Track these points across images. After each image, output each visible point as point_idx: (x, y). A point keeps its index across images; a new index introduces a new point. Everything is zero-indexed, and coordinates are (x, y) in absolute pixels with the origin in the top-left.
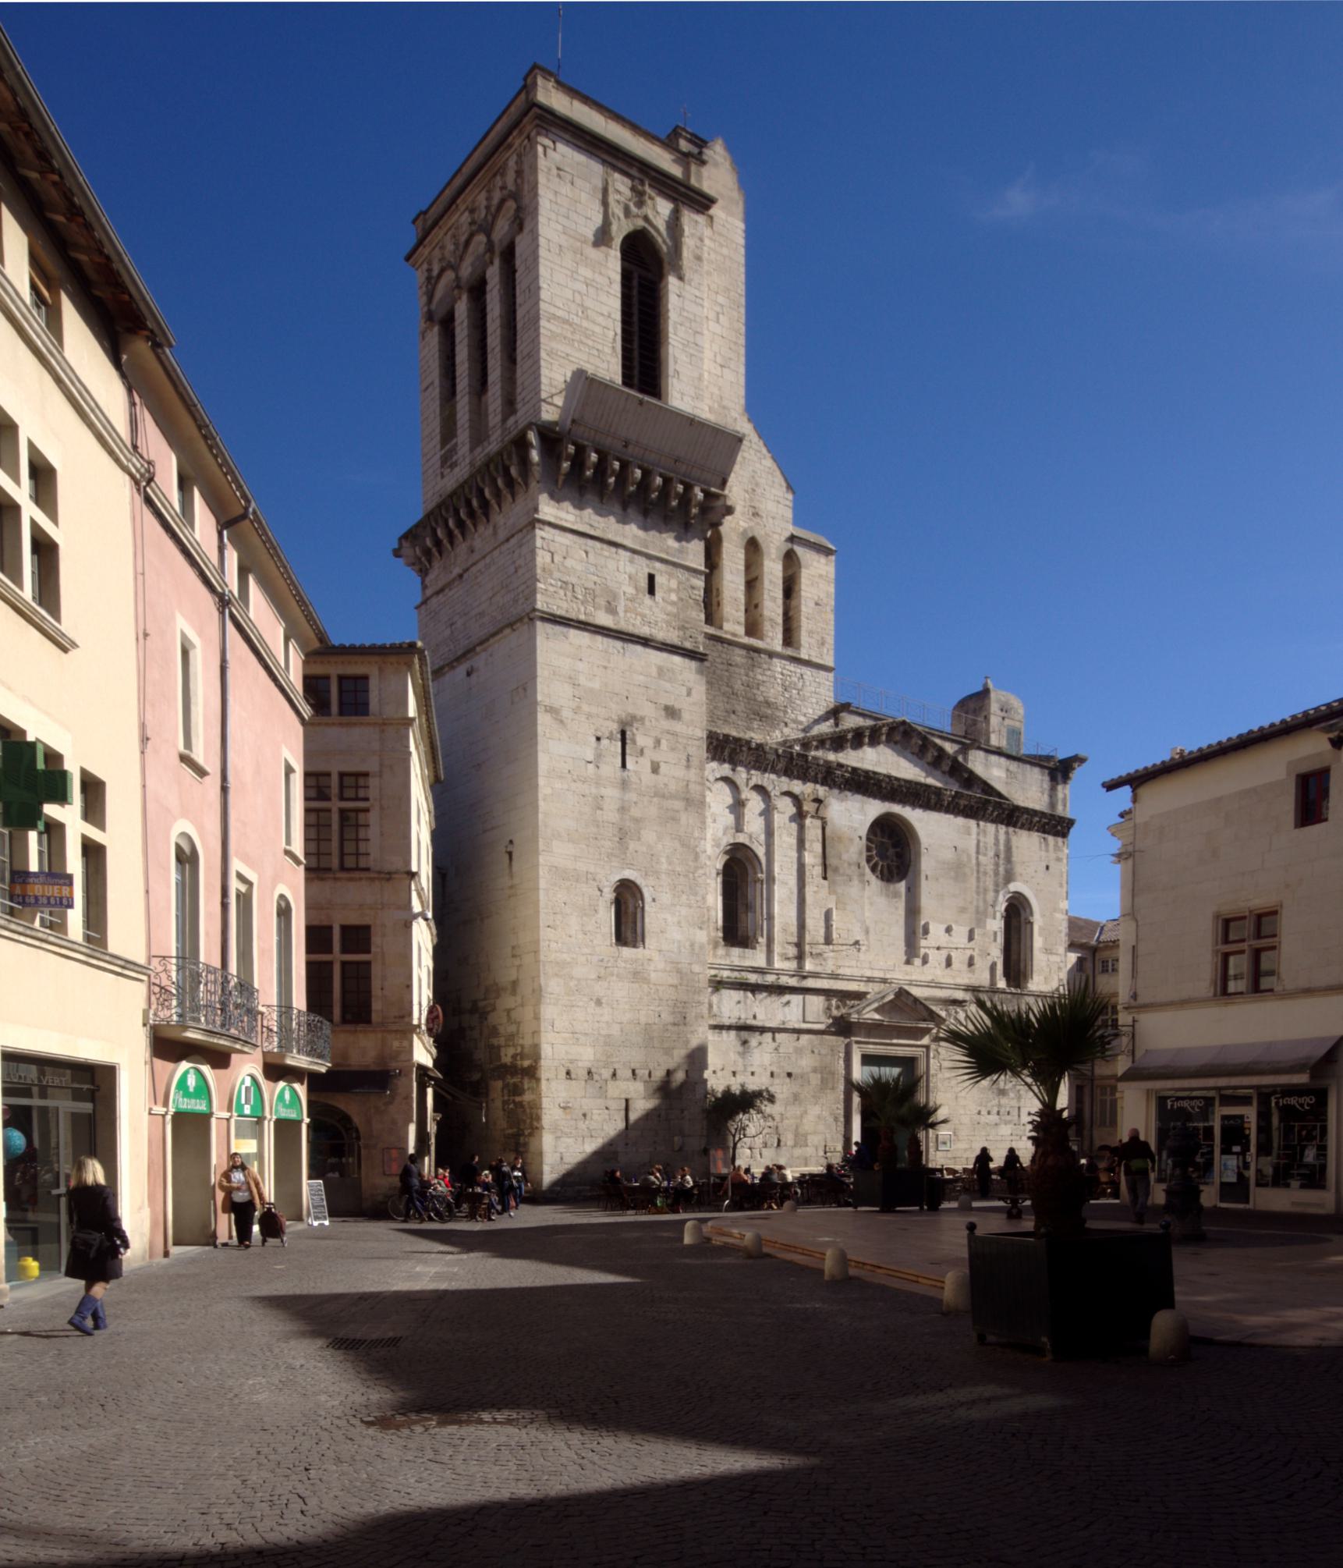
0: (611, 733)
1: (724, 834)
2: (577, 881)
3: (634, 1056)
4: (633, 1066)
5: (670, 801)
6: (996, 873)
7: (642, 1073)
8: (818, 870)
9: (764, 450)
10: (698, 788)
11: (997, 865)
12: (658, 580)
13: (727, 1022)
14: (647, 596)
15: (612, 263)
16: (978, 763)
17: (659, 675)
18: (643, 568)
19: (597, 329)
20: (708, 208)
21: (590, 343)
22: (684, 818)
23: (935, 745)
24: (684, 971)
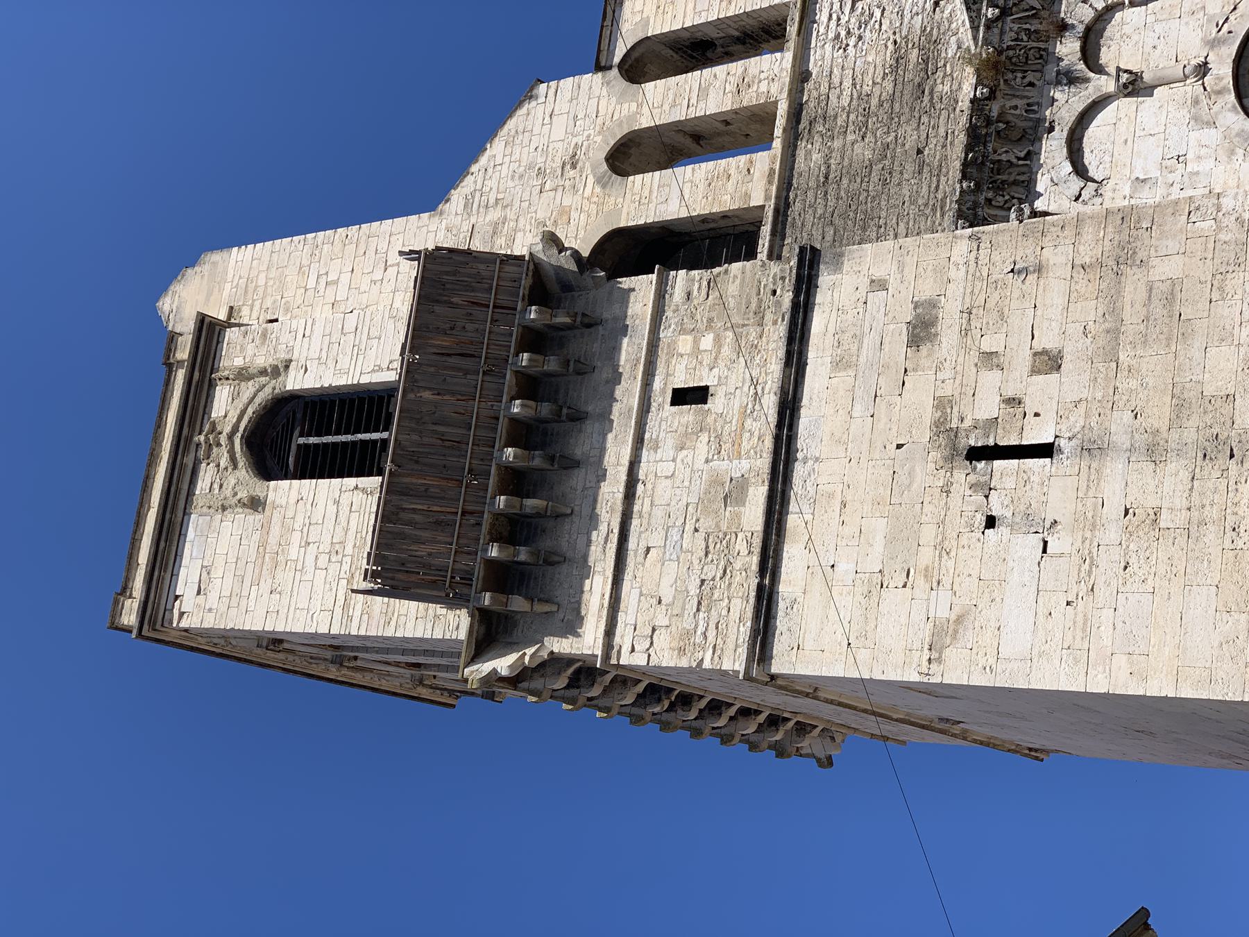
5: (1126, 315)
10: (1088, 232)
12: (682, 380)
15: (284, 491)
17: (848, 366)
18: (666, 418)
22: (1164, 269)
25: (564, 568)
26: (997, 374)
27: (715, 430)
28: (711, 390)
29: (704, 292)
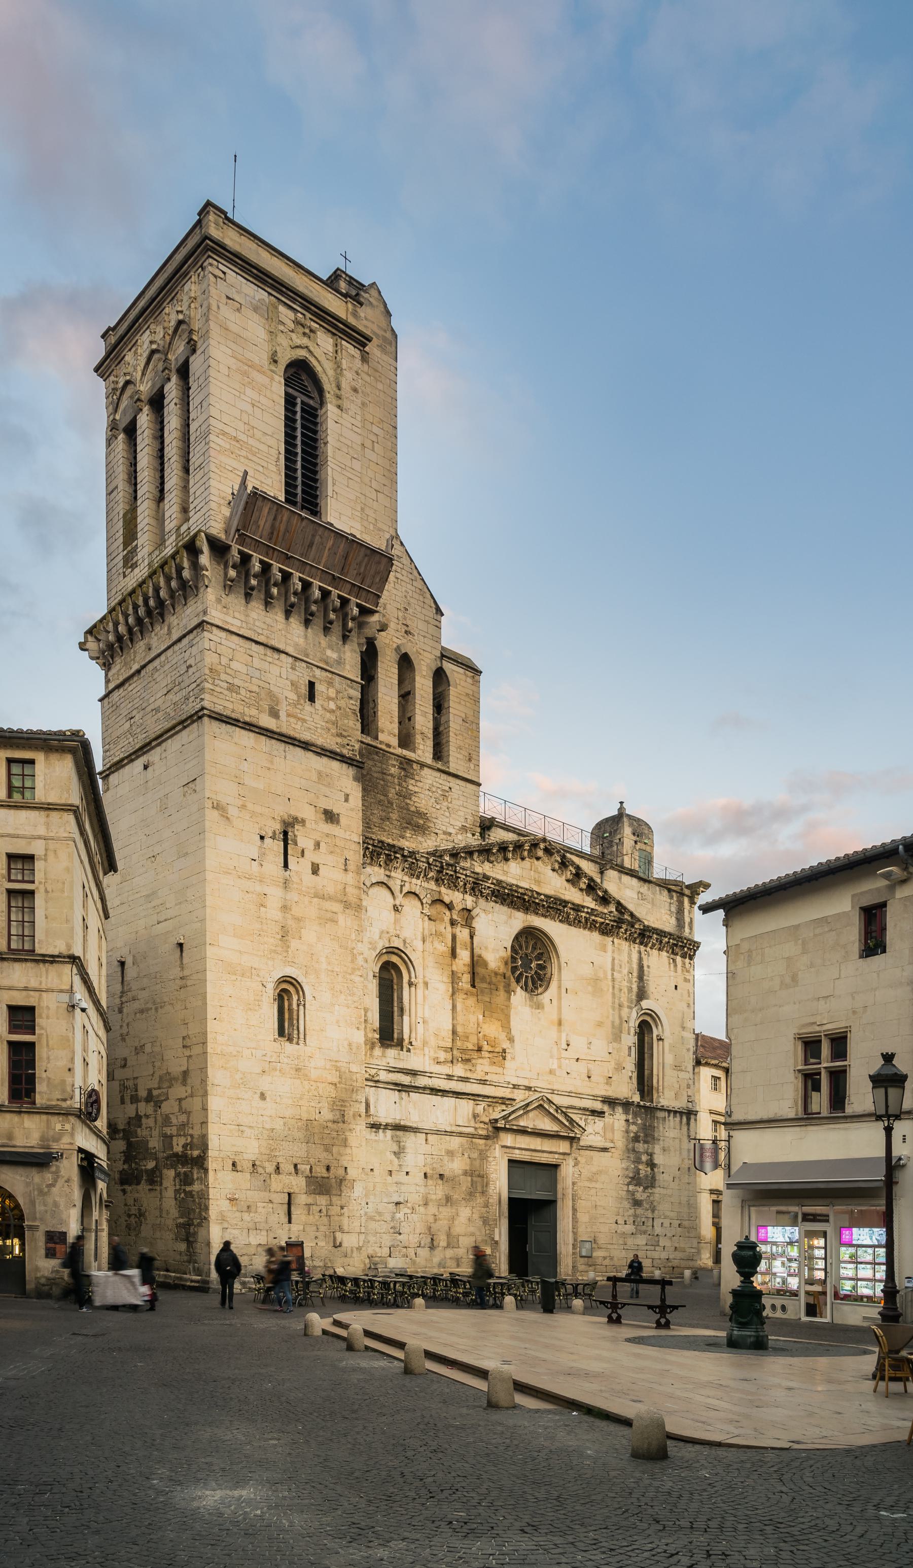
0: (274, 832)
2: (243, 975)
3: (298, 1151)
4: (295, 1161)
10: (356, 891)
12: (319, 688)
13: (383, 1121)
14: (308, 703)
22: (341, 918)
24: (343, 1069)
25: (243, 601)
26: (313, 848)
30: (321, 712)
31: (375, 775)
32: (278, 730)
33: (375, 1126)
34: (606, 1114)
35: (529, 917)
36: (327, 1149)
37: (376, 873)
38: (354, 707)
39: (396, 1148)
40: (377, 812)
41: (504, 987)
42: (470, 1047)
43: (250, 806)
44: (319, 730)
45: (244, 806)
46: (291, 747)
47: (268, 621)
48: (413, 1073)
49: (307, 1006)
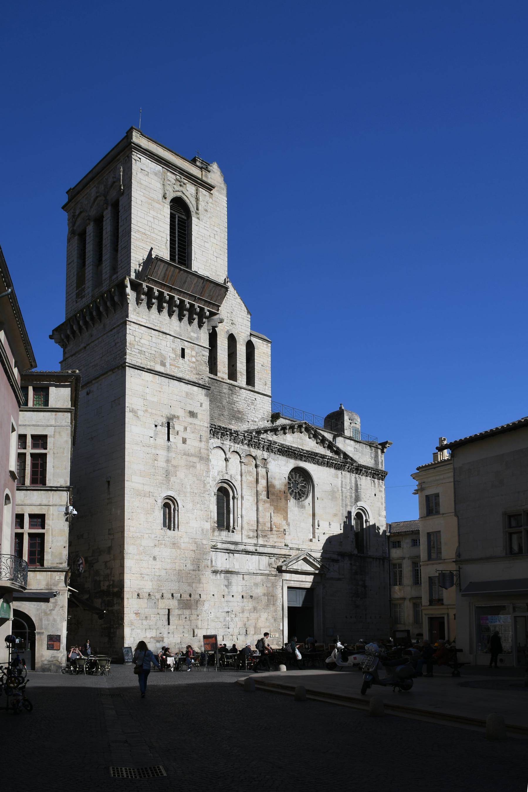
0: (162, 423)
1: (218, 475)
3: (173, 587)
6: (351, 497)
7: (177, 595)
8: (265, 493)
9: (237, 295)
10: (206, 452)
11: (351, 493)
12: (186, 351)
16: (340, 443)
19: (159, 238)
20: (211, 190)
21: (154, 243)
22: (198, 465)
23: (321, 434)
24: (199, 543)
27: (176, 359)
28: (184, 359)
29: (203, 360)
30: (188, 363)
31: (216, 393)
32: (165, 372)
33: (215, 572)
34: (340, 561)
35: (297, 462)
36: (190, 585)
37: (216, 442)
38: (205, 360)
39: (226, 583)
40: (217, 412)
41: (285, 497)
42: (267, 529)
43: (150, 410)
44: (187, 372)
45: (146, 411)
46: (172, 380)
47: (160, 319)
48: (236, 543)
49: (179, 511)
